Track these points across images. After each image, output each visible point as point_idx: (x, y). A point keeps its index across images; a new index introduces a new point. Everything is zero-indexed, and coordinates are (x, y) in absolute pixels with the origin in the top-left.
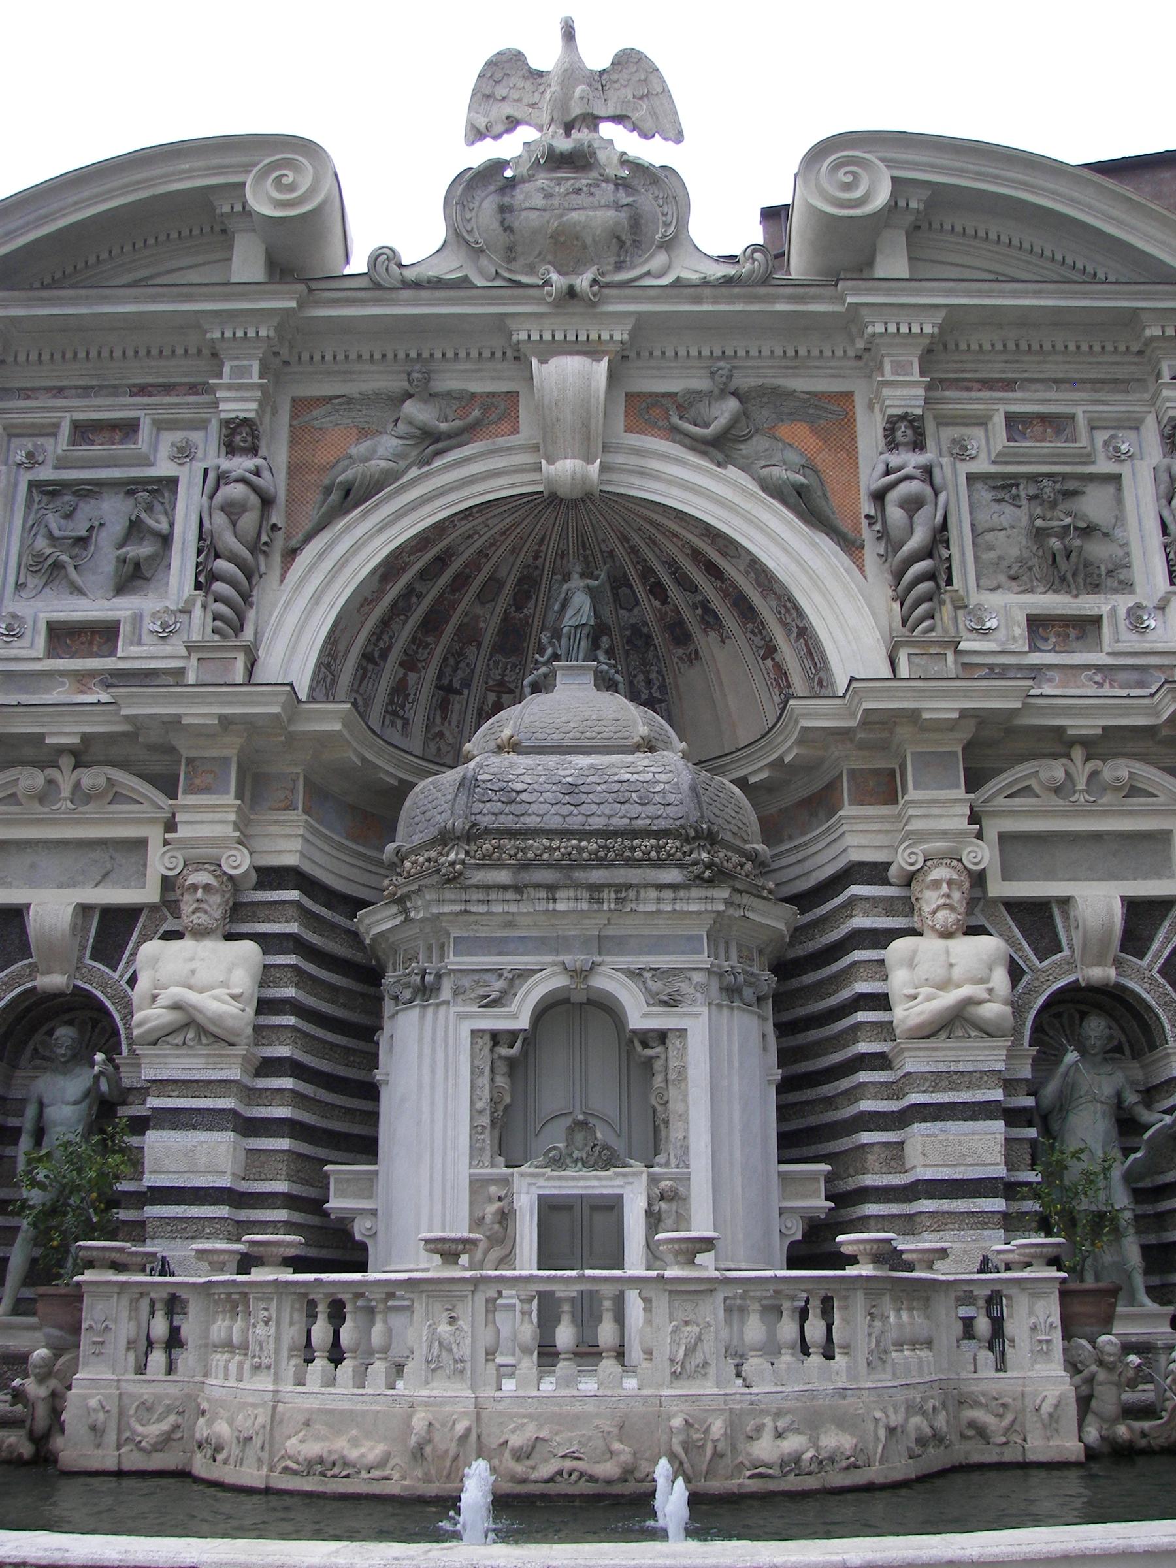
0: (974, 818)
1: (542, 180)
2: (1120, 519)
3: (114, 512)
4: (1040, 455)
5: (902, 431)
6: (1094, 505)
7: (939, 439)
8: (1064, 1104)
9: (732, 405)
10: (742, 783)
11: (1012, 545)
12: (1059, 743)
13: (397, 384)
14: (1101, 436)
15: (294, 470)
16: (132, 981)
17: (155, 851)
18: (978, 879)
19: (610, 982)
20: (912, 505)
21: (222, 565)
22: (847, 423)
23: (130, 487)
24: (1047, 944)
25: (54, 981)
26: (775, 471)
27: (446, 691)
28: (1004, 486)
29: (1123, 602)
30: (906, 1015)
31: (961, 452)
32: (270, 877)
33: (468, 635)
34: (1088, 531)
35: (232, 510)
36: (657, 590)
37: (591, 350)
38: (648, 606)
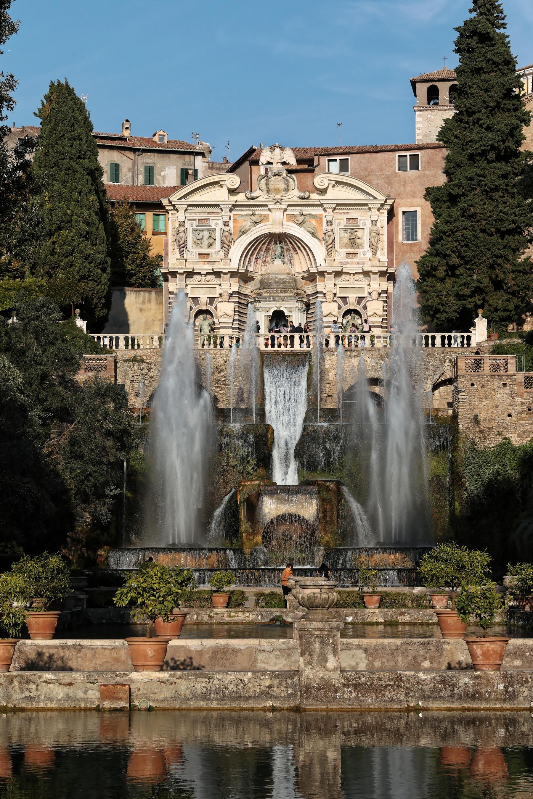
0: (335, 285)
1: (273, 178)
2: (363, 236)
3: (206, 234)
4: (351, 226)
5: (329, 223)
6: (359, 234)
7: (335, 222)
9: (303, 218)
11: (346, 241)
12: (348, 273)
13: (250, 213)
14: (362, 222)
15: (234, 227)
16: (216, 308)
17: (217, 289)
20: (329, 236)
21: (225, 245)
22: (321, 219)
23: (209, 230)
24: (345, 303)
25: (204, 308)
26: (309, 229)
27: (257, 259)
28: (346, 230)
29: (362, 250)
31: (339, 224)
32: (234, 292)
34: (359, 238)
35: (226, 237)
36: (291, 243)
38: (290, 245)
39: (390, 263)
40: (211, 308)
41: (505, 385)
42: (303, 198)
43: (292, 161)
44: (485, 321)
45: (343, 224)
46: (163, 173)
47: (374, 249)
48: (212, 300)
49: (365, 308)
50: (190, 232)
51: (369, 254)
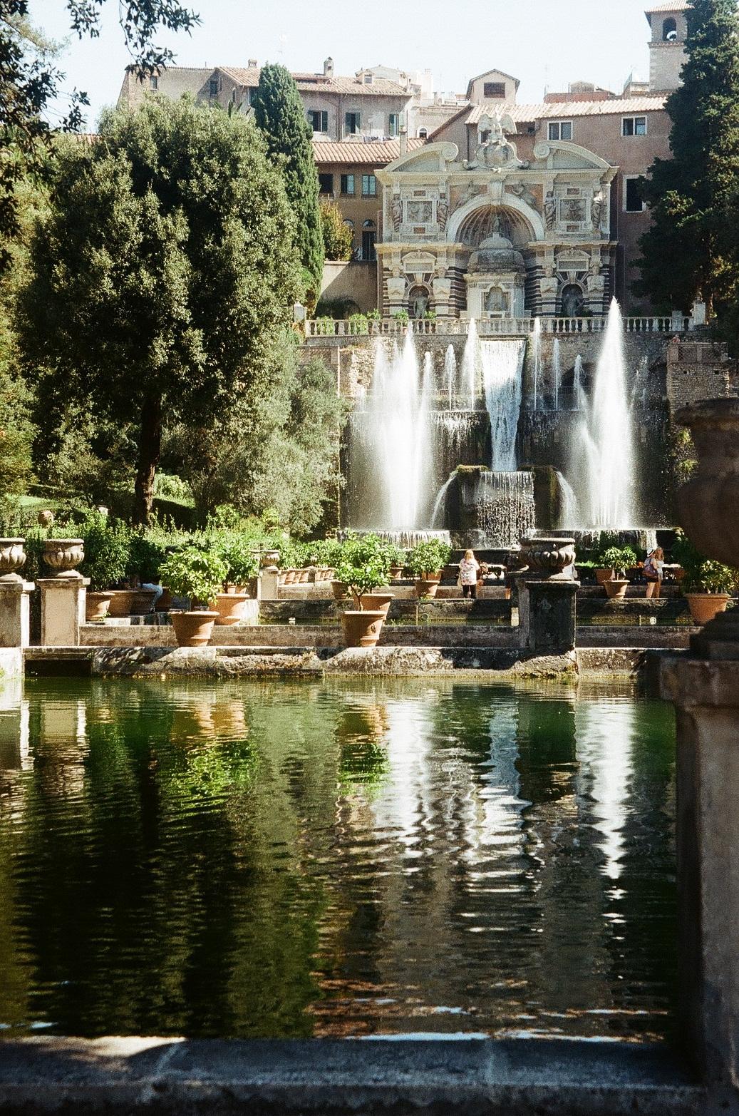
0: (555, 259)
3: (422, 207)
4: (573, 197)
8: (568, 301)
10: (521, 251)
11: (566, 212)
16: (432, 284)
18: (555, 269)
19: (500, 285)
23: (425, 202)
25: (419, 285)
27: (474, 231)
29: (583, 222)
30: (542, 289)
33: (478, 222)
37: (497, 181)
39: (613, 238)
40: (427, 285)
41: (717, 373)
42: (522, 168)
43: (514, 130)
44: (703, 306)
45: (565, 196)
46: (370, 121)
47: (597, 221)
48: (427, 277)
49: (585, 282)
50: (405, 204)
51: (591, 227)
